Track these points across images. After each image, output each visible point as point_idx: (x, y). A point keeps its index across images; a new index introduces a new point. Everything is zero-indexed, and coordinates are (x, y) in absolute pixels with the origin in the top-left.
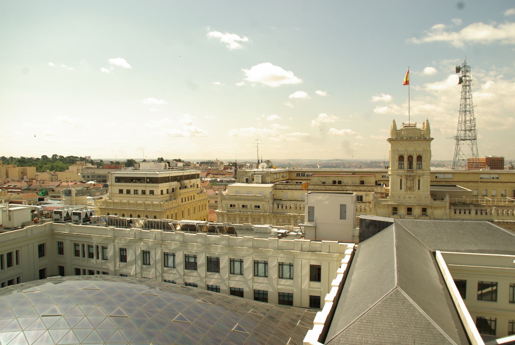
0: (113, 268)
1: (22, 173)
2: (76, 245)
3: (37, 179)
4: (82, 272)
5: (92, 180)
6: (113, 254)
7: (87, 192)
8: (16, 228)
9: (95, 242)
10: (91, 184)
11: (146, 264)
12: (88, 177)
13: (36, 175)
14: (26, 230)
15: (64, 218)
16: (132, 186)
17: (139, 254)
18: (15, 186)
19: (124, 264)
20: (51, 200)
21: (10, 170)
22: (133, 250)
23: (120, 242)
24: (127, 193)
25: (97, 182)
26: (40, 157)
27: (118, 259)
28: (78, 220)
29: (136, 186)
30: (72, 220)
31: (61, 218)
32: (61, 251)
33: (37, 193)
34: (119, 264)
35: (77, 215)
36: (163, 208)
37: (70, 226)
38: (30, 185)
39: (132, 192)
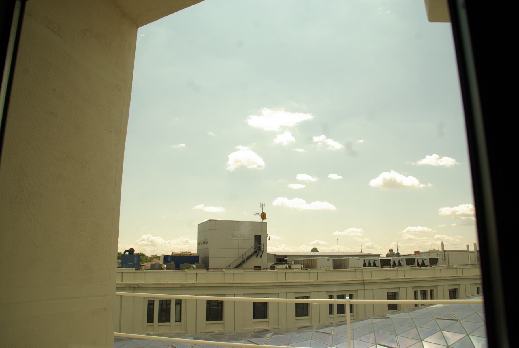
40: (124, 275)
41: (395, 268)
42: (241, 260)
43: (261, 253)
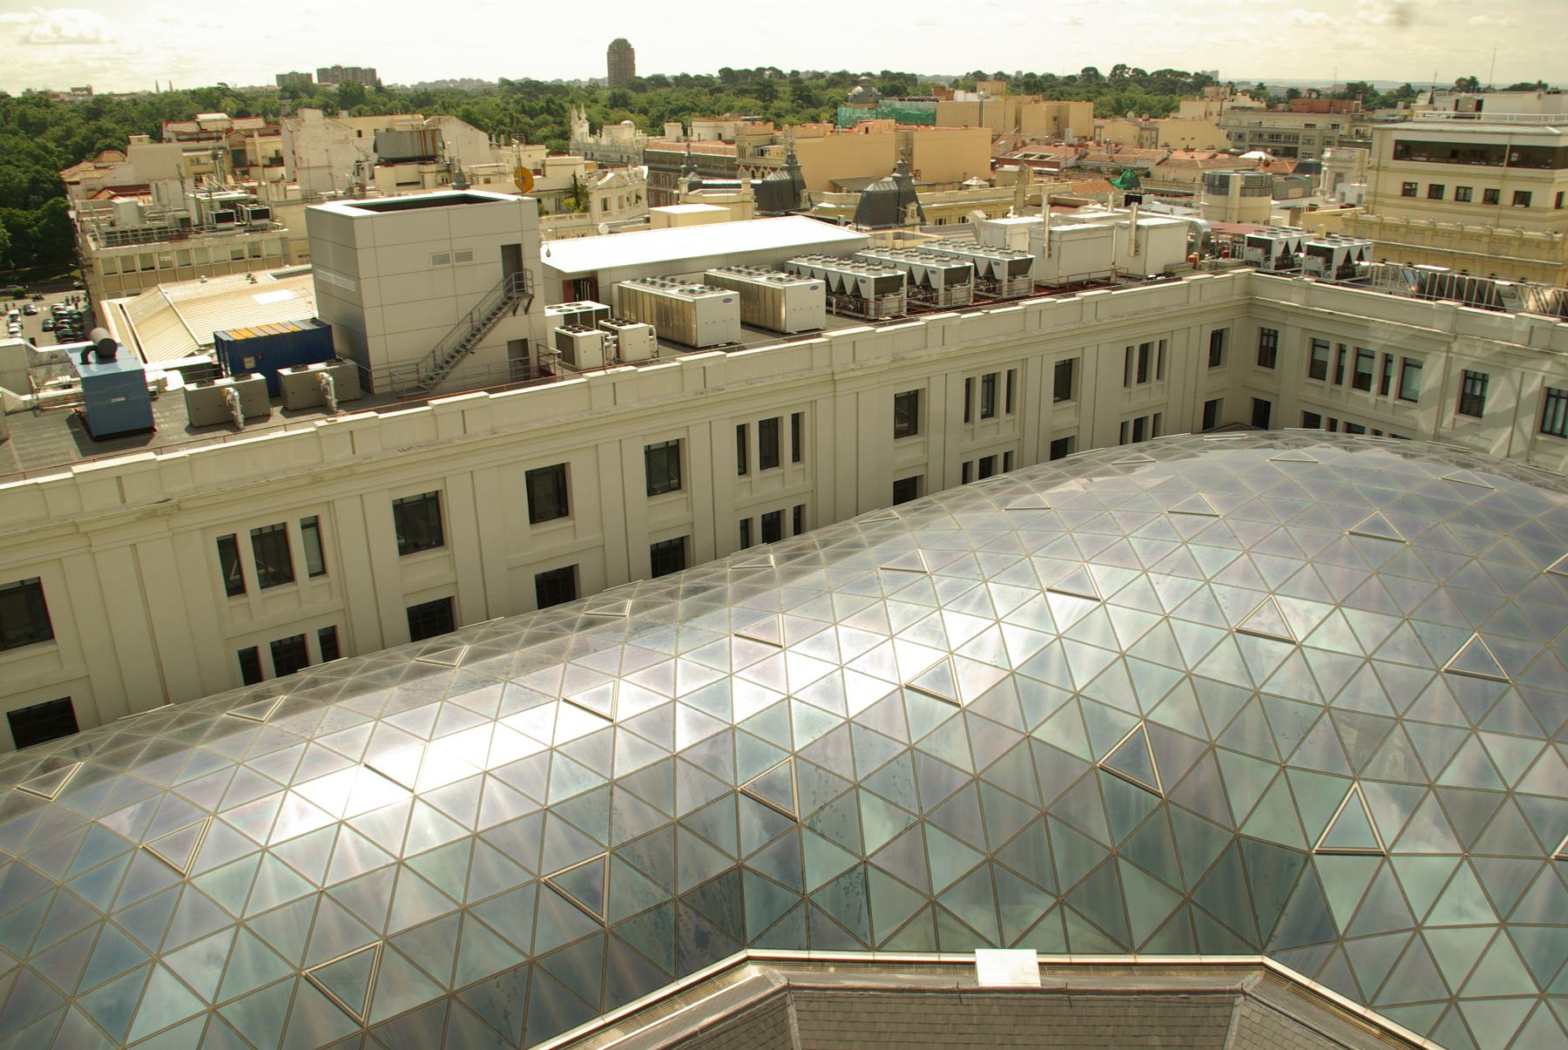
0: (1433, 427)
1: (1055, 119)
2: (1315, 345)
3: (1097, 139)
4: (1324, 422)
5: (1252, 148)
6: (1440, 383)
7: (1257, 186)
8: (1152, 281)
9: (1377, 342)
10: (1260, 159)
11: (1551, 433)
12: (1240, 137)
13: (1096, 127)
14: (1188, 286)
15: (1277, 259)
16: (1451, 175)
17: (1531, 394)
18: (1042, 157)
19: (1468, 419)
20: (1162, 202)
21: (1025, 110)
22: (1511, 381)
23: (1467, 351)
24: (1430, 197)
25: (1275, 153)
26: (1105, 72)
27: (1452, 403)
28: (1322, 269)
29: (1468, 175)
30: (1303, 269)
31: (1268, 259)
32: (1267, 356)
33: (1106, 179)
34: (1455, 419)
35: (1319, 255)
36: (1559, 256)
37: (1309, 287)
38: (1082, 157)
39: (1449, 194)
40: (124, 482)
41: (919, 320)
42: (465, 329)
43: (525, 302)
